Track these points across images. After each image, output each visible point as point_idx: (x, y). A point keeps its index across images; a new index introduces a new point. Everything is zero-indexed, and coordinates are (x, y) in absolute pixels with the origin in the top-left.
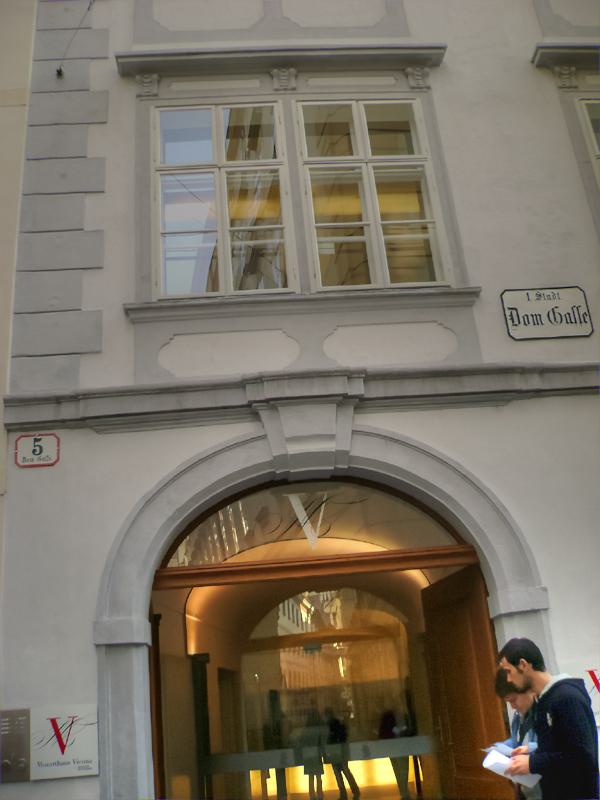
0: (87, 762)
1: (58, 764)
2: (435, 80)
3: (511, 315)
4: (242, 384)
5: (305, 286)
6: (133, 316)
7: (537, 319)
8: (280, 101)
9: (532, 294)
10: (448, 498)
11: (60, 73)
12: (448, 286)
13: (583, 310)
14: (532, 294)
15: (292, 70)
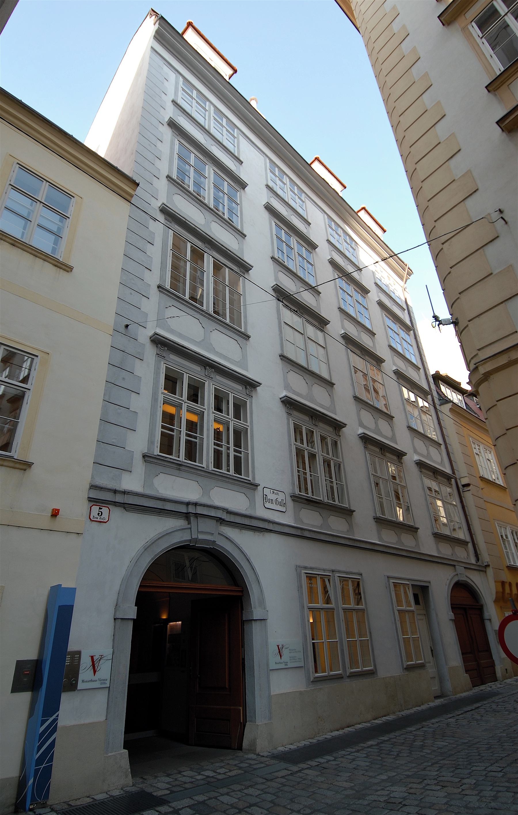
0: (105, 680)
1: (92, 681)
3: (265, 498)
4: (188, 504)
6: (146, 459)
9: (272, 490)
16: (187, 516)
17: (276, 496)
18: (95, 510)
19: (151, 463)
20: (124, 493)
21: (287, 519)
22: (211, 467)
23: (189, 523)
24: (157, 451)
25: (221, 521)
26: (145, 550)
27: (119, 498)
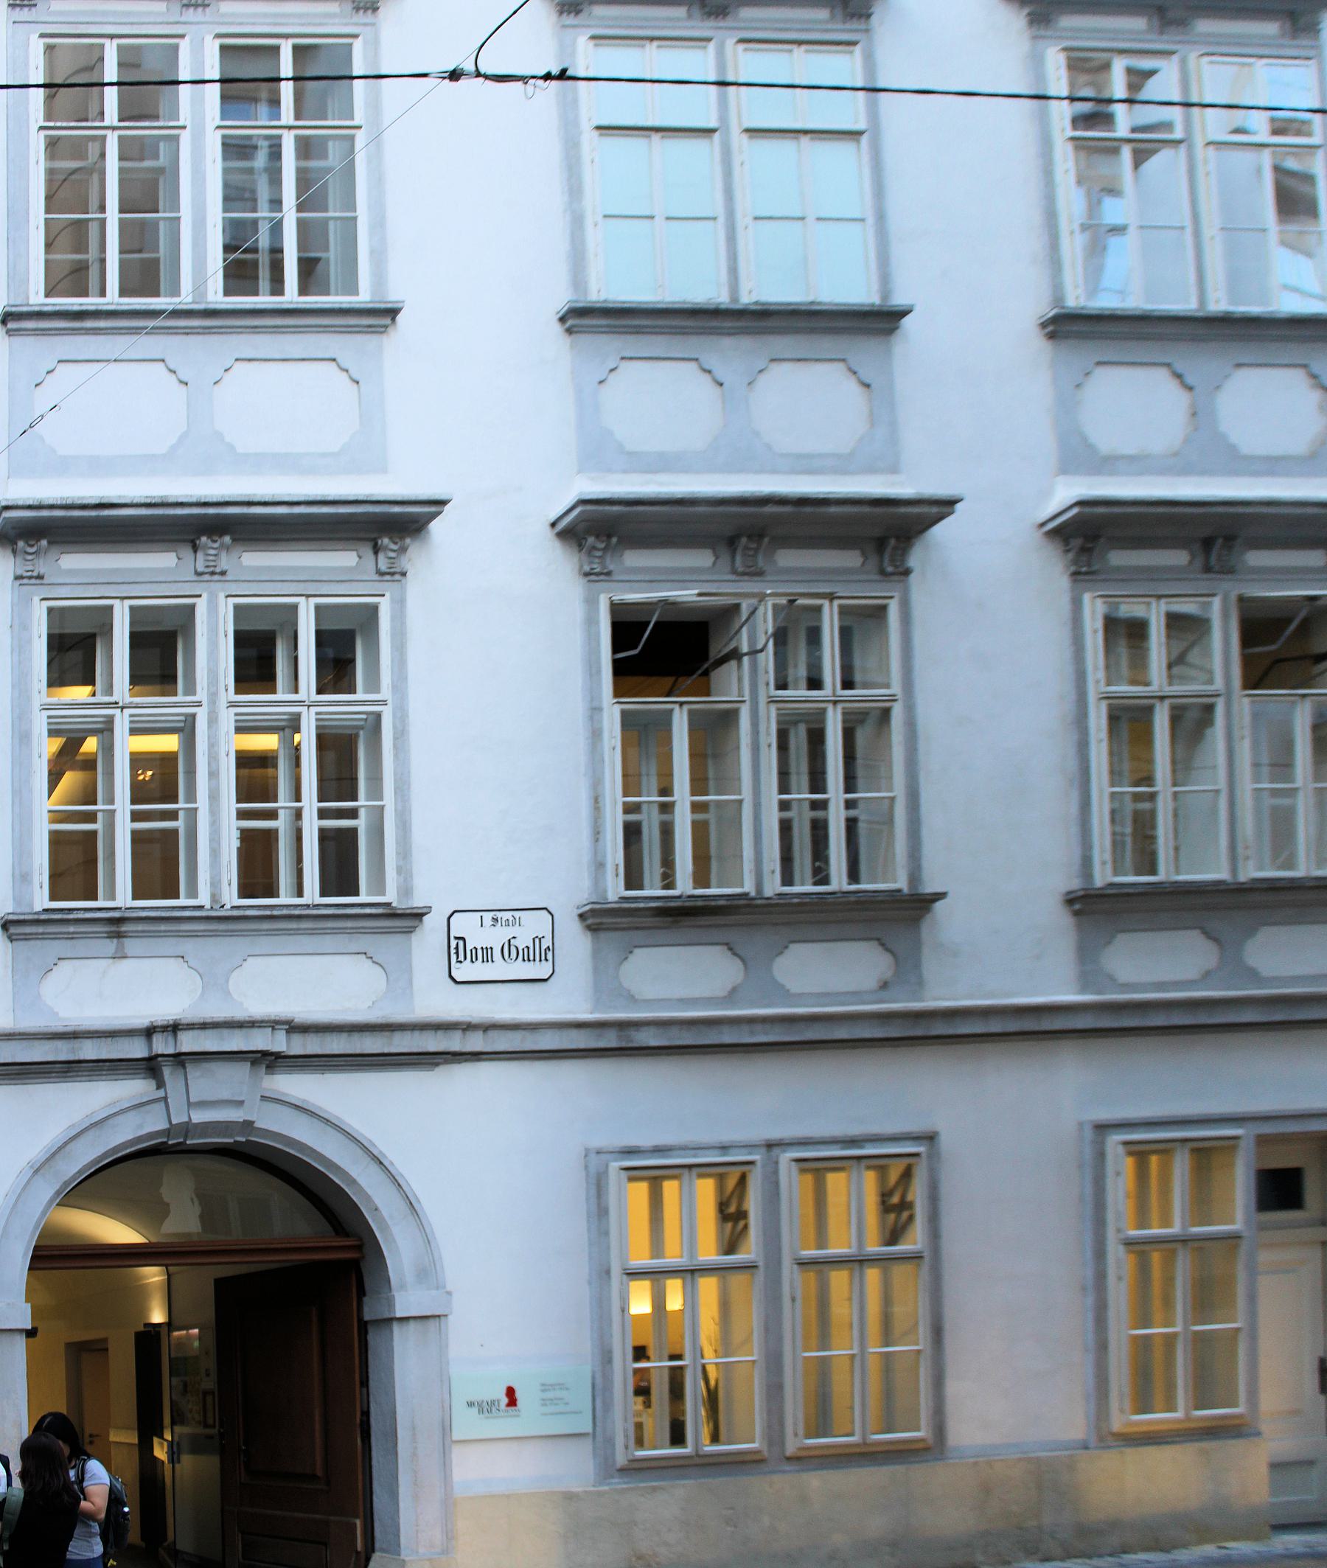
4: (149, 1032)
7: (487, 954)
12: (389, 904)
16: (150, 1067)
19: (26, 938)
22: (231, 896)
23: (161, 1084)
24: (41, 900)
25: (270, 1061)
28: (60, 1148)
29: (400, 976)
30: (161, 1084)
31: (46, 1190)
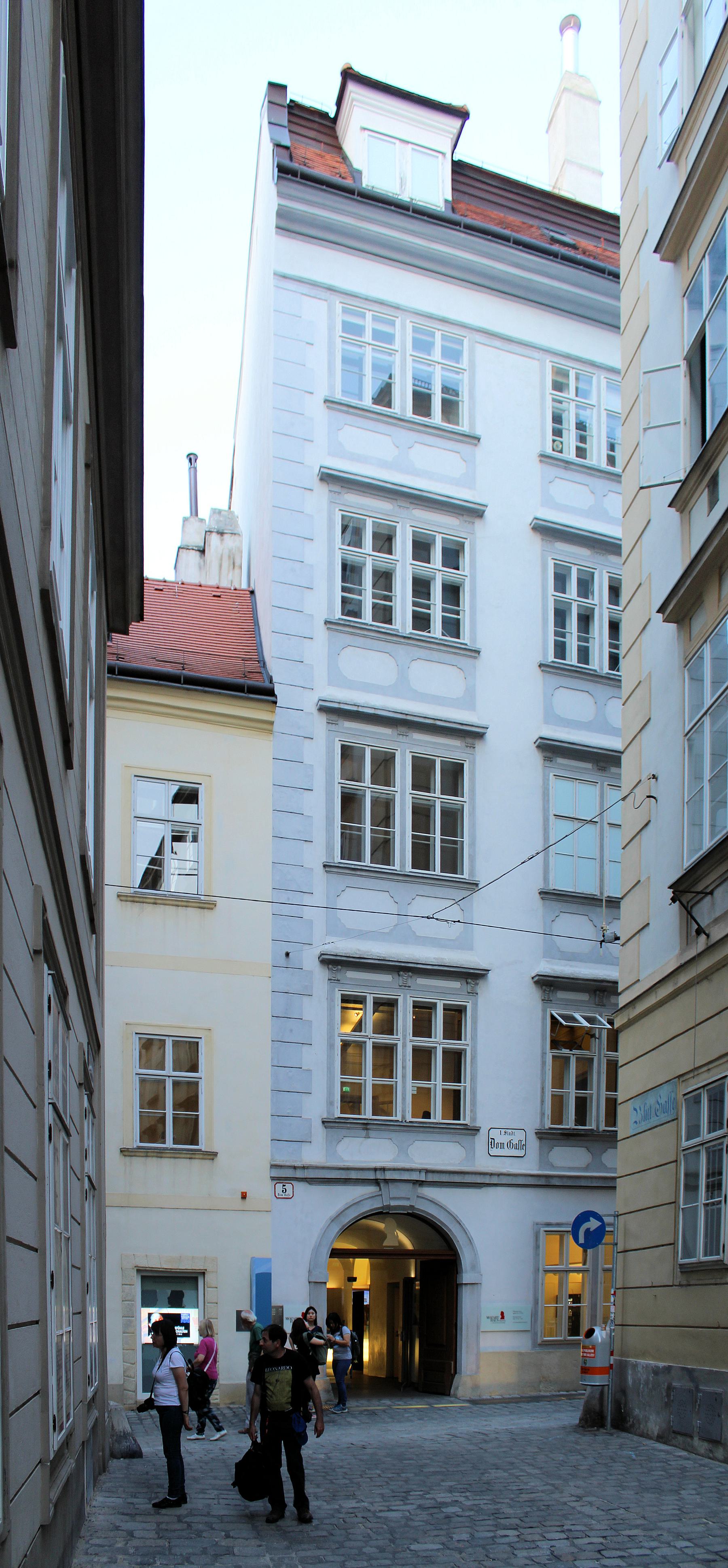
2: (479, 745)
4: (375, 1170)
5: (403, 1117)
6: (326, 1124)
8: (402, 995)
9: (503, 1131)
10: (450, 1230)
11: (287, 954)
12: (466, 1125)
13: (523, 1143)
14: (503, 1132)
15: (410, 974)
16: (376, 1182)
17: (511, 1137)
18: (279, 1187)
19: (332, 1127)
20: (304, 1168)
21: (529, 1166)
23: (380, 1189)
24: (337, 1113)
25: (421, 1183)
26: (333, 1221)
27: (299, 1174)
28: (342, 1212)
29: (471, 1152)
30: (380, 1189)
31: (336, 1229)
